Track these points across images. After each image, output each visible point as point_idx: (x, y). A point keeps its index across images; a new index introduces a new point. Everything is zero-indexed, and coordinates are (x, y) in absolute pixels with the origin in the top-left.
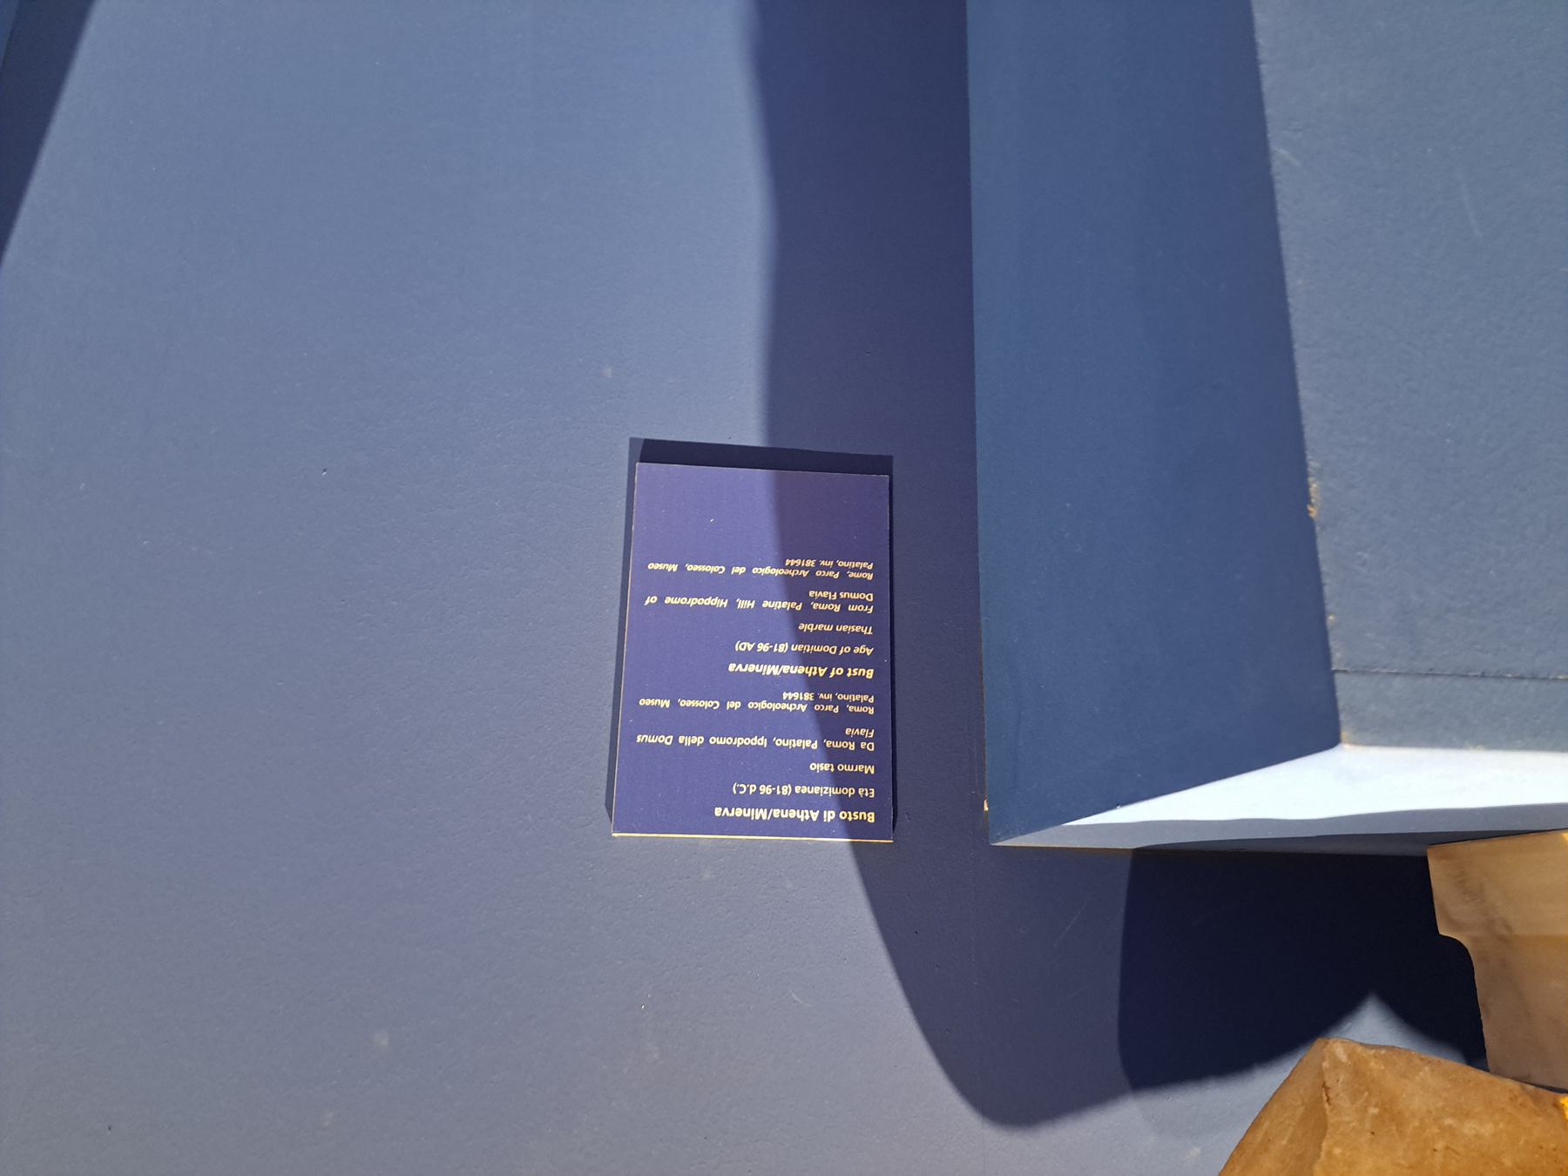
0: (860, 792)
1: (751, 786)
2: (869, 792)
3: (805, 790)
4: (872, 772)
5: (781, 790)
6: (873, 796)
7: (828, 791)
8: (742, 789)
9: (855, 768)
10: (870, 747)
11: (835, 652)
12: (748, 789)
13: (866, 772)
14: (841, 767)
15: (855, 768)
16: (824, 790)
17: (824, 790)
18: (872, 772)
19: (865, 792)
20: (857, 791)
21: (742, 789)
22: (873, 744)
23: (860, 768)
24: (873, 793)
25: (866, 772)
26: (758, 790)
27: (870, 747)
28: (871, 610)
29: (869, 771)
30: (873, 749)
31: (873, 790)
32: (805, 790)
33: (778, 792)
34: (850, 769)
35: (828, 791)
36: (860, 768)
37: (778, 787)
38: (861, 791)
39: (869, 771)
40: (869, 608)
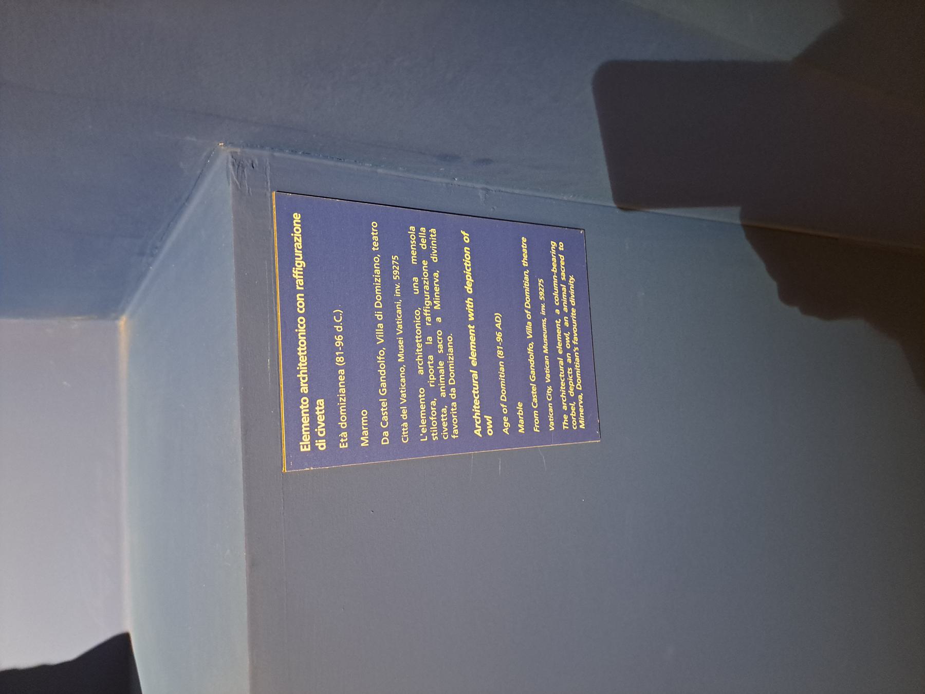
0: (344, 433)
1: (341, 327)
2: (345, 442)
3: (342, 379)
4: (362, 445)
5: (340, 356)
6: (341, 447)
7: (342, 402)
8: (338, 319)
9: (365, 427)
12: (338, 324)
15: (365, 427)
16: (343, 397)
17: (343, 397)
18: (362, 445)
19: (344, 438)
20: (344, 430)
21: (338, 319)
23: (366, 433)
24: (344, 446)
26: (338, 334)
31: (347, 446)
32: (342, 379)
33: (337, 353)
35: (342, 402)
37: (343, 353)
38: (344, 434)
40: (538, 429)
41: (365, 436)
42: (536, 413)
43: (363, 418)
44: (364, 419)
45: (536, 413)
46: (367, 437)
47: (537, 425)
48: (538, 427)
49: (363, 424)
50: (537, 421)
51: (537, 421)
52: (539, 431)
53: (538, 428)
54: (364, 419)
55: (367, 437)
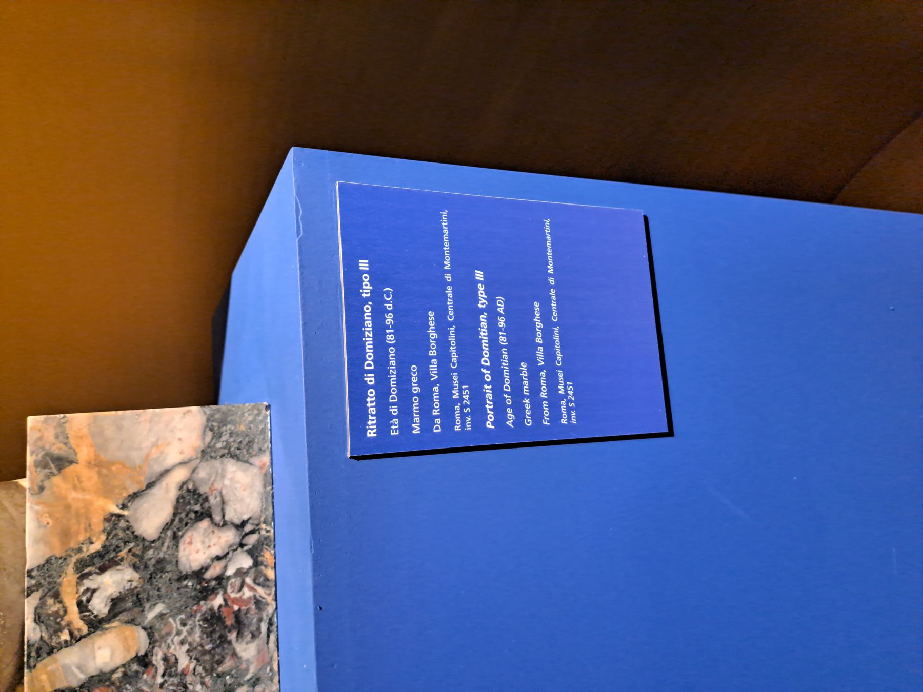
9: (416, 413)
10: (437, 428)
11: (505, 389)
13: (413, 425)
14: (416, 400)
15: (416, 413)
18: (414, 432)
22: (440, 430)
23: (417, 419)
25: (414, 425)
27: (437, 428)
28: (546, 423)
29: (415, 429)
30: (435, 431)
34: (415, 408)
36: (417, 419)
39: (415, 429)
41: (416, 423)
42: (545, 404)
43: (414, 405)
44: (416, 406)
45: (545, 404)
46: (419, 425)
47: (546, 417)
48: (548, 419)
49: (415, 411)
50: (546, 413)
51: (546, 413)
52: (549, 424)
53: (547, 420)
54: (416, 406)
55: (419, 425)
